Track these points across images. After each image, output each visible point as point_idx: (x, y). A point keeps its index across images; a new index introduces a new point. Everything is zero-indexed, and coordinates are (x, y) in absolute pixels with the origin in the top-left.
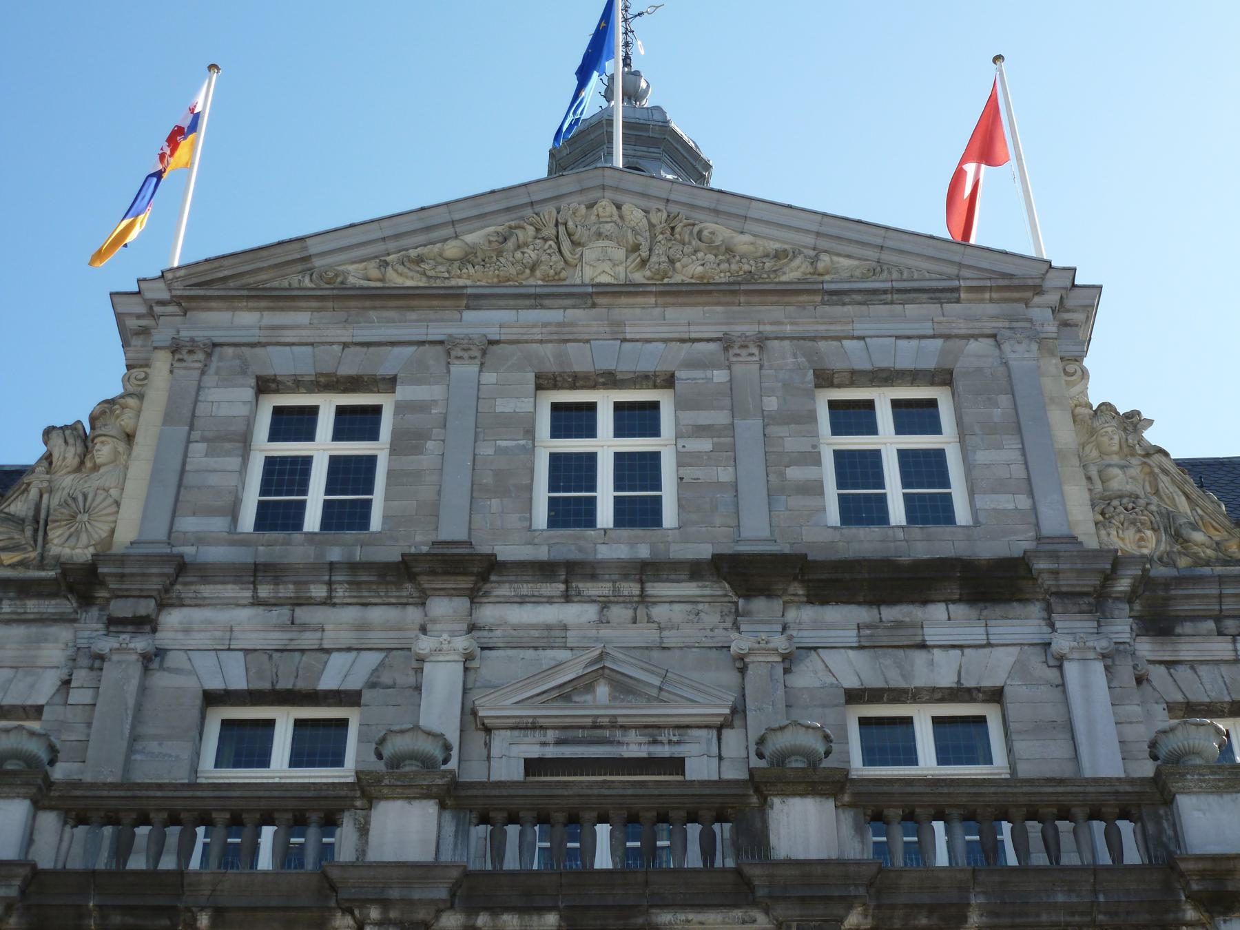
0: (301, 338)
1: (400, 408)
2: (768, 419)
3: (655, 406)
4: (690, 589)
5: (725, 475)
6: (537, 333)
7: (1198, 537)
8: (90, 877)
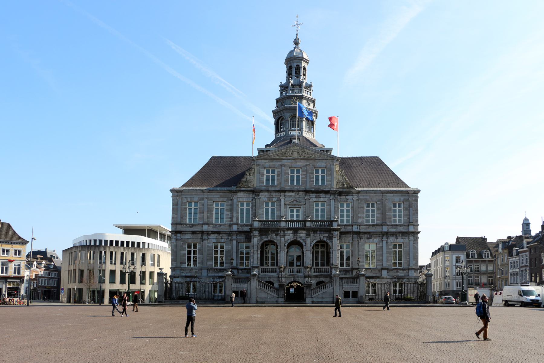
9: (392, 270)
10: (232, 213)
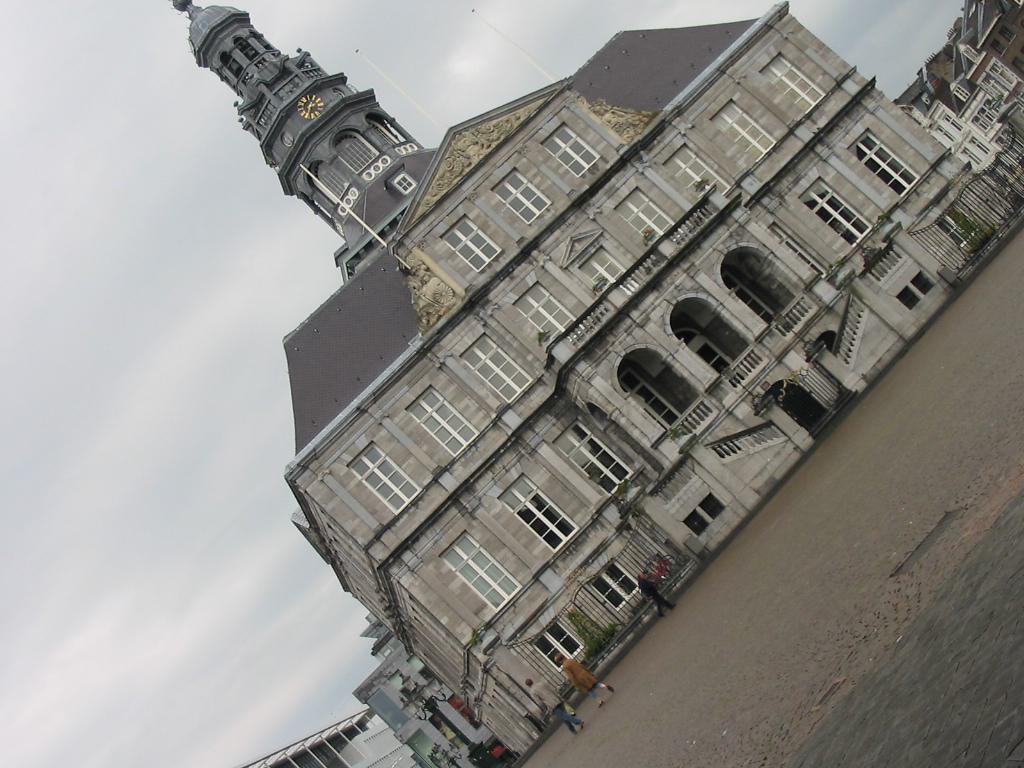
9: (906, 201)
10: (472, 394)
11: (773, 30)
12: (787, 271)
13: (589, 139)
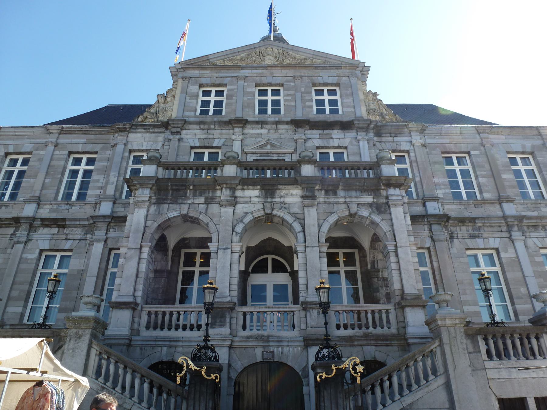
0: (208, 76)
1: (228, 90)
2: (302, 93)
3: (279, 90)
4: (286, 127)
5: (293, 104)
6: (256, 75)
7: (387, 117)
8: (169, 179)
10: (108, 176)
11: (539, 137)
12: (395, 273)
13: (345, 101)
